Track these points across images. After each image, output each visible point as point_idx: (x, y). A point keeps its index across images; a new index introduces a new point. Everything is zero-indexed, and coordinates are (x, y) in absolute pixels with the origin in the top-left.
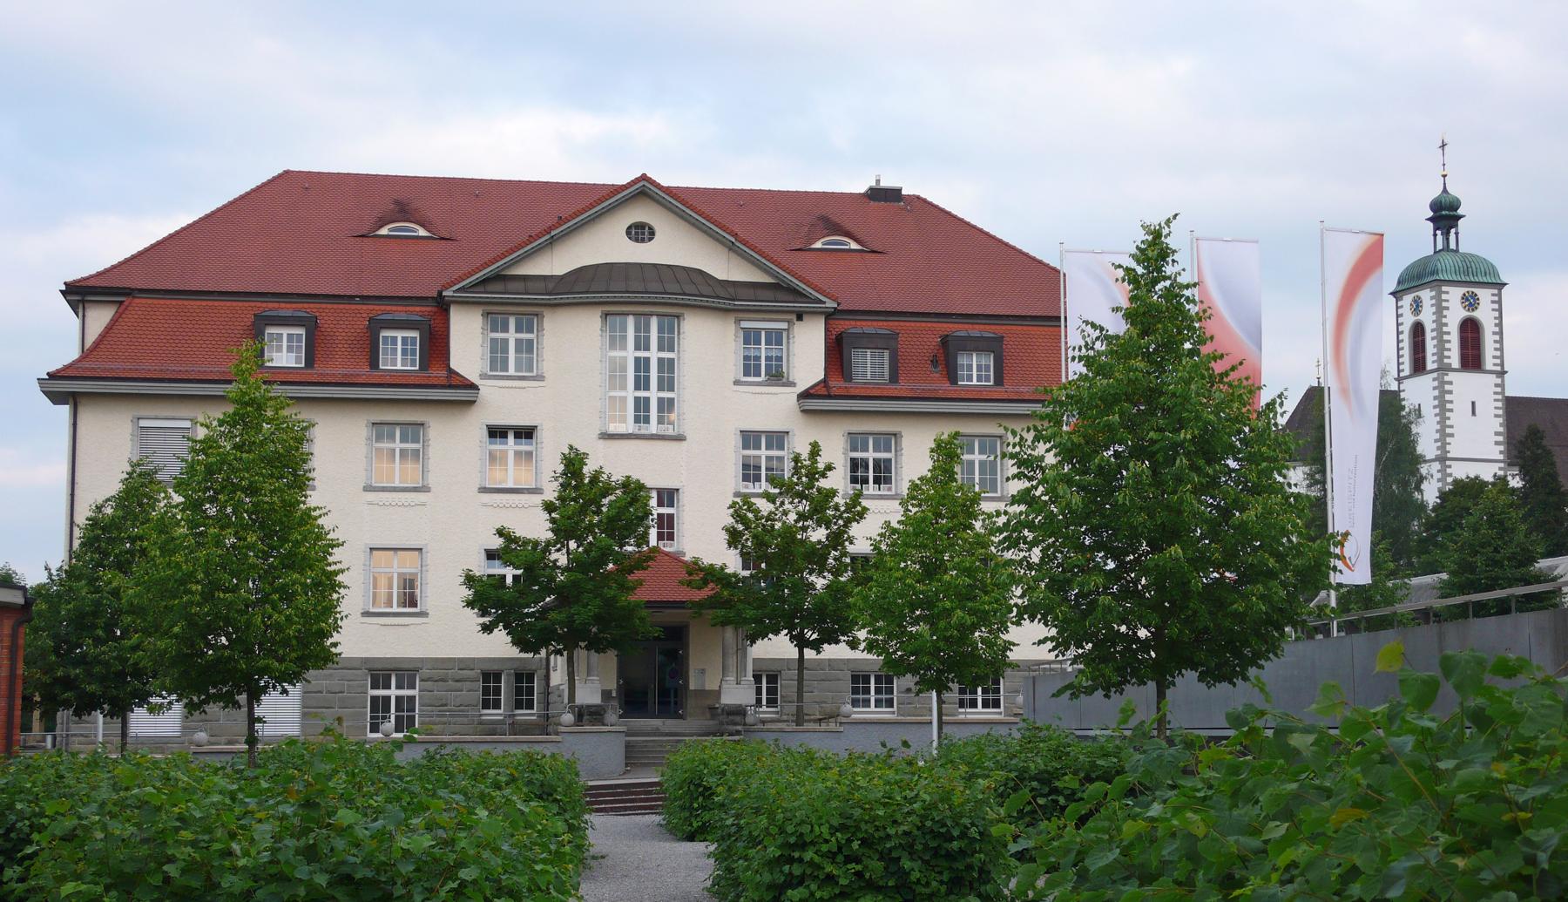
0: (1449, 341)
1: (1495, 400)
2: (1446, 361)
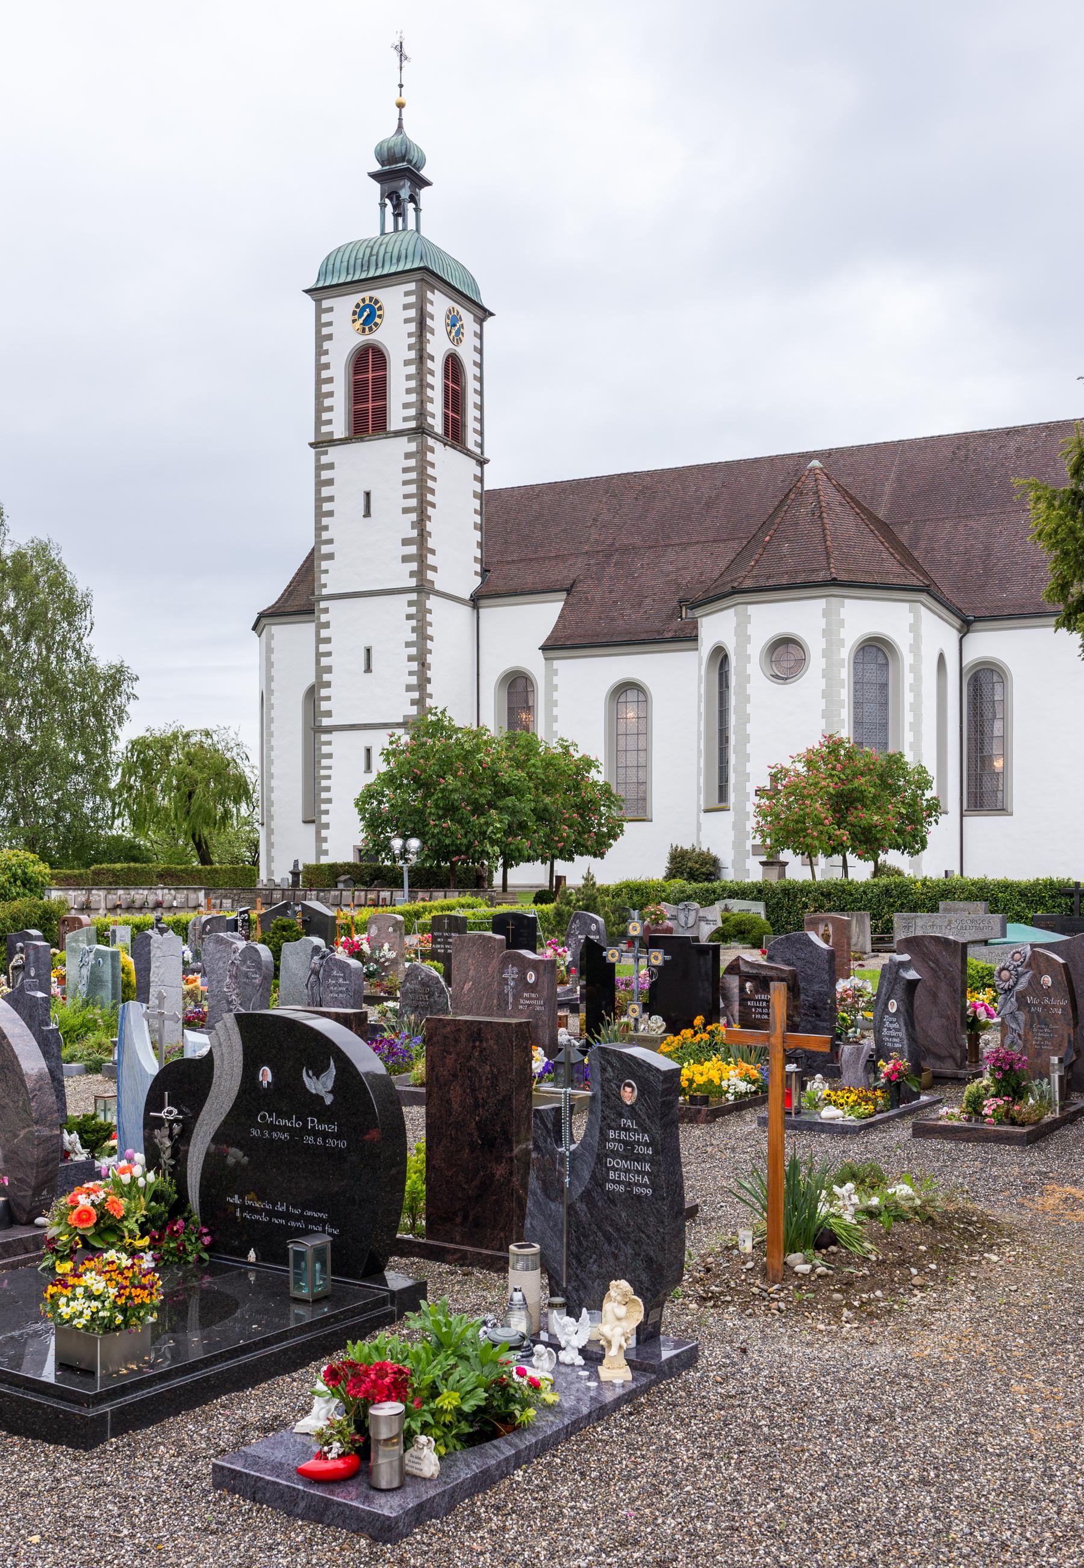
0: (330, 394)
1: (405, 483)
2: (325, 429)
